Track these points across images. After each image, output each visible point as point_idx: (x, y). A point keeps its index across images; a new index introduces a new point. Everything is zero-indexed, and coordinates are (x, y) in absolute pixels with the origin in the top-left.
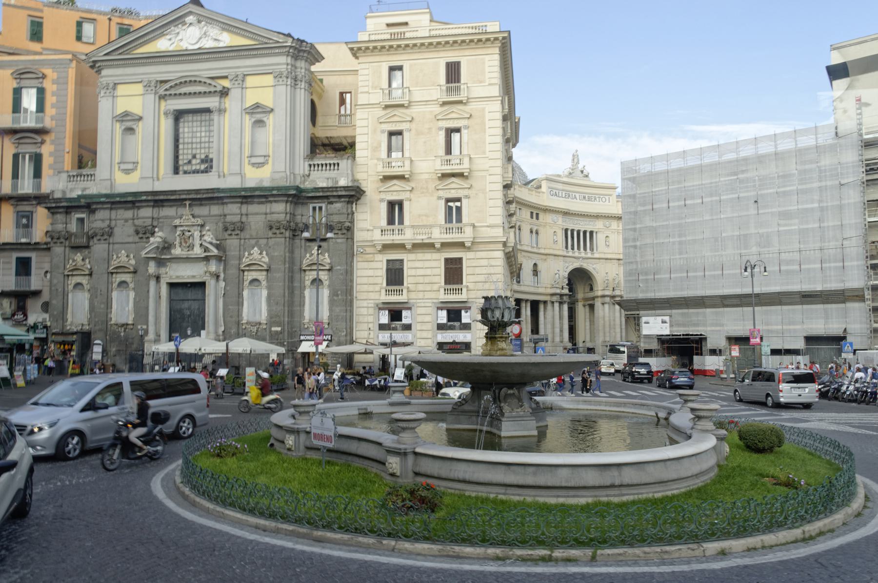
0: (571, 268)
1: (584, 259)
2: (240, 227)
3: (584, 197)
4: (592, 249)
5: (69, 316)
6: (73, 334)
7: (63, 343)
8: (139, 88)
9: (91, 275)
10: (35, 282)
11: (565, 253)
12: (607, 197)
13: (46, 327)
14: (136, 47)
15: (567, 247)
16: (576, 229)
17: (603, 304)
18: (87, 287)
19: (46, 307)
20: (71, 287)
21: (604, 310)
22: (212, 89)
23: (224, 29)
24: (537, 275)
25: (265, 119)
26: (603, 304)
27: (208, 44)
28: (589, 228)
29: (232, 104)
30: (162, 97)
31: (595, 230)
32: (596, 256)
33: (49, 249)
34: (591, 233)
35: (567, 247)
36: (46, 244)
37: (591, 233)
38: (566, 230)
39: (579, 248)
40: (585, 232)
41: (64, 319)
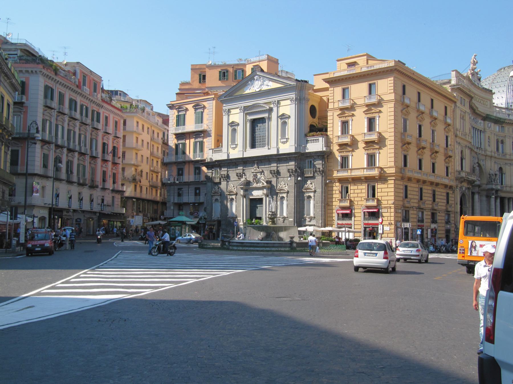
2: (277, 174)
5: (213, 214)
6: (215, 221)
7: (210, 225)
8: (238, 111)
9: (221, 195)
10: (202, 199)
13: (205, 218)
14: (236, 92)
18: (219, 201)
19: (205, 210)
20: (214, 201)
22: (265, 109)
23: (270, 81)
25: (287, 121)
27: (265, 88)
29: (274, 115)
30: (247, 114)
33: (206, 184)
36: (205, 181)
41: (212, 215)
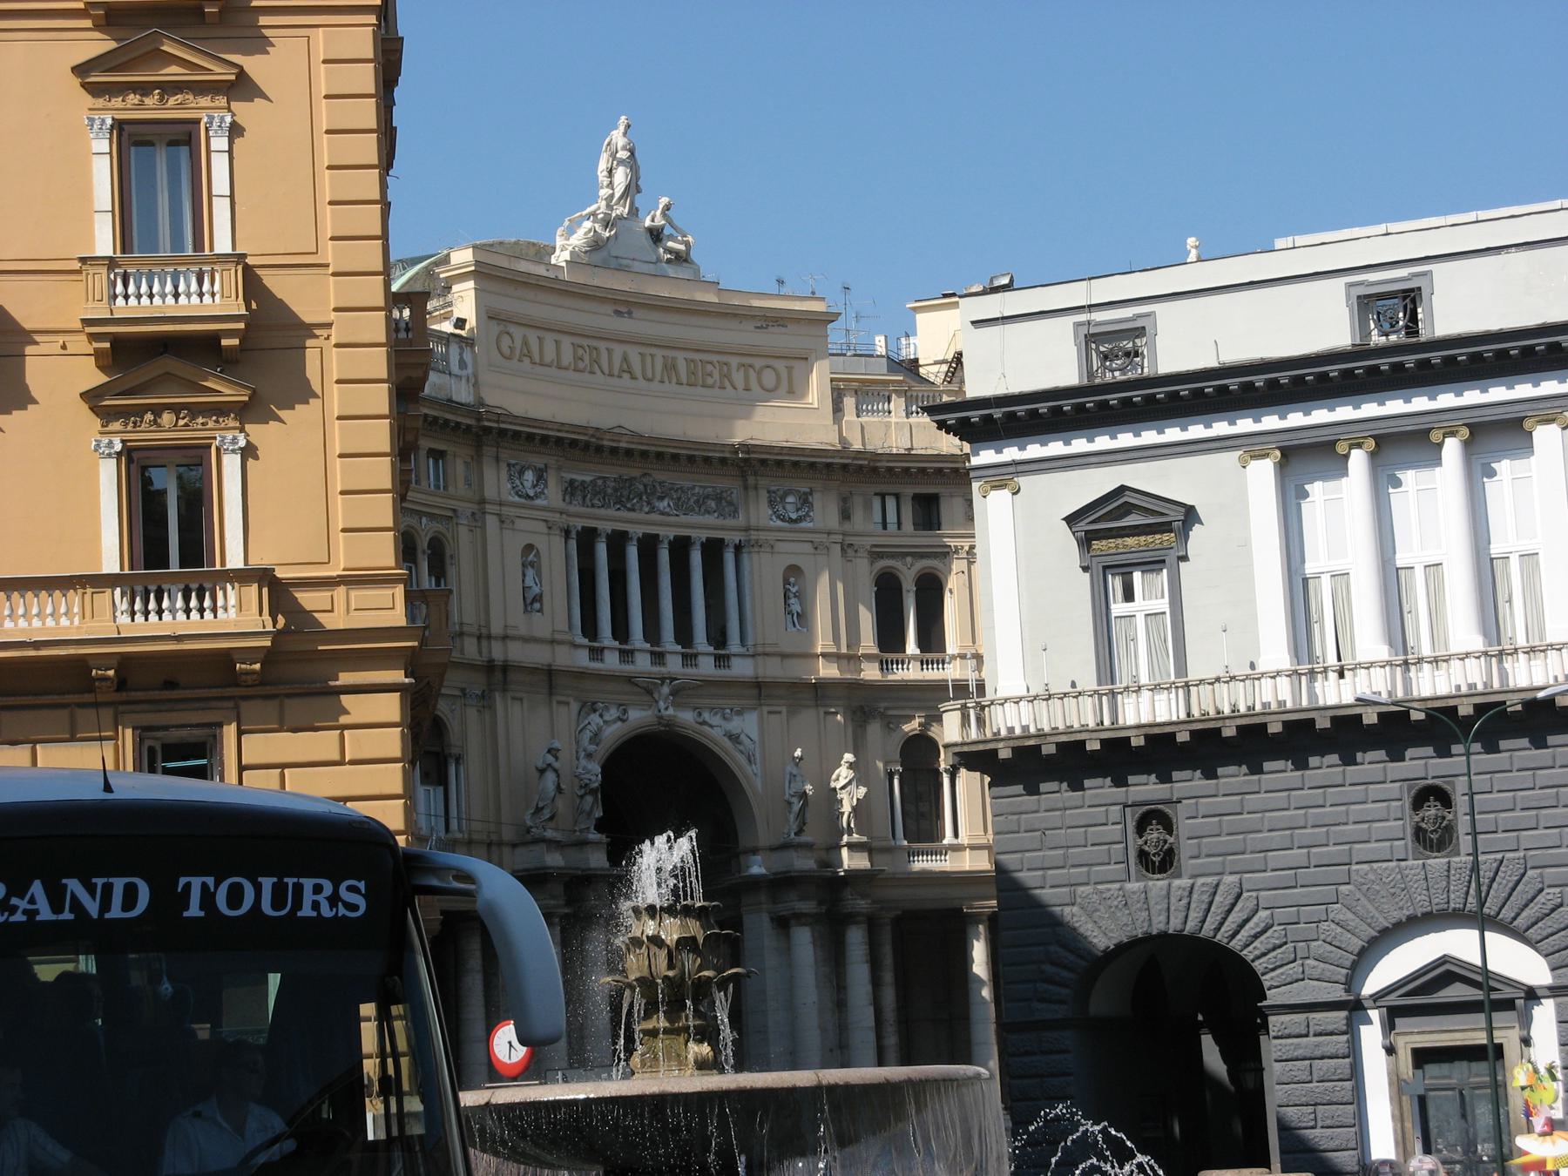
0: (613, 733)
1: (682, 692)
3: (670, 367)
4: (718, 637)
11: (582, 660)
12: (780, 365)
15: (590, 627)
16: (637, 531)
17: (783, 924)
21: (787, 950)
24: (442, 780)
26: (783, 924)
28: (701, 526)
31: (732, 537)
32: (741, 668)
34: (713, 550)
35: (590, 627)
37: (713, 550)
38: (587, 539)
39: (652, 631)
40: (680, 547)
